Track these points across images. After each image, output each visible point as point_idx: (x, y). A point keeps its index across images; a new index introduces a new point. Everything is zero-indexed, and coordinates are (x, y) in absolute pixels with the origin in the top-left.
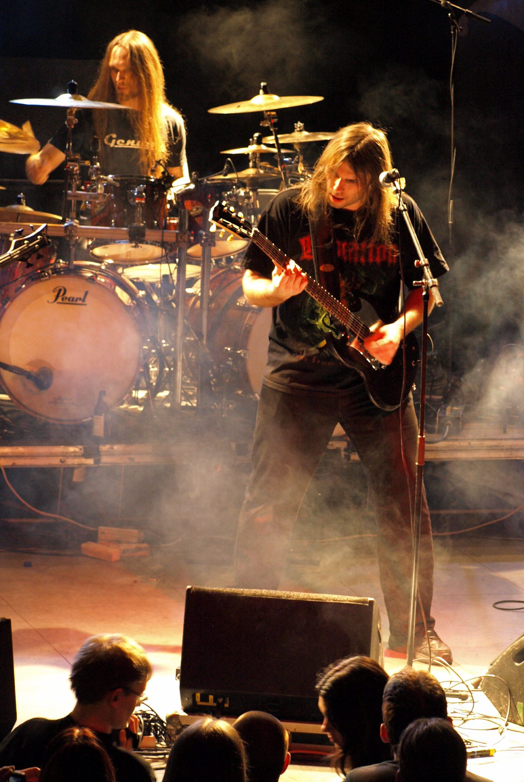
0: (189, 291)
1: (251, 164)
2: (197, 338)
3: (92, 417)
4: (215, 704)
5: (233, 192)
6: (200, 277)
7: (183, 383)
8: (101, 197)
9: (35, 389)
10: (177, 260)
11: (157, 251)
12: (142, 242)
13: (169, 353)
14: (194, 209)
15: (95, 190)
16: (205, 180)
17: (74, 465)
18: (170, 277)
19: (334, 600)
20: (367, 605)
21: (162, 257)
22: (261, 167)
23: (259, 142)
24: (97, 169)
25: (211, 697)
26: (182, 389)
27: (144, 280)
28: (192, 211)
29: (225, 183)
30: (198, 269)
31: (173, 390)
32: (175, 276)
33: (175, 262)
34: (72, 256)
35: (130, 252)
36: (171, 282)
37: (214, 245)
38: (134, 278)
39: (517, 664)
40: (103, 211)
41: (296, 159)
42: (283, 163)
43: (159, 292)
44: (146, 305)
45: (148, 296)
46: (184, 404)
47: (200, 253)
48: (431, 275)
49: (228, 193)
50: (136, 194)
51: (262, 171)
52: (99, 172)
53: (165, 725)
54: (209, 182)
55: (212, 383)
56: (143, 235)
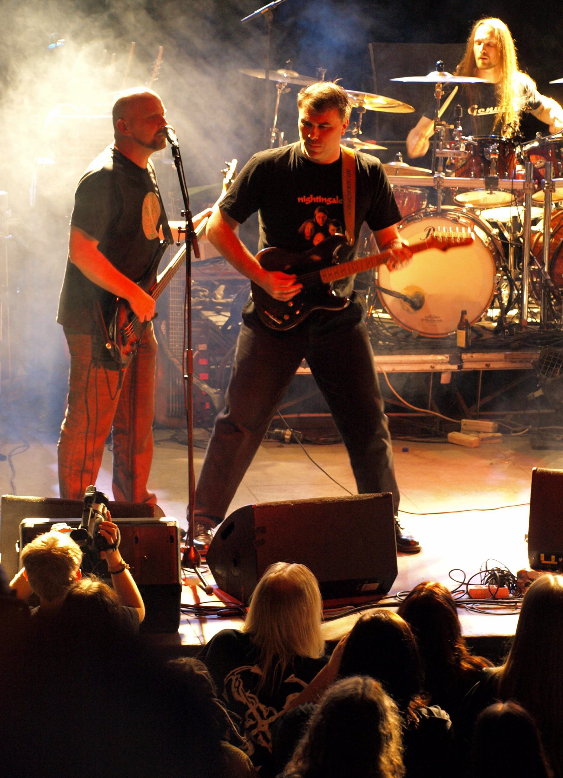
0: (534, 228)
2: (540, 267)
3: (456, 331)
4: (556, 563)
6: (543, 217)
7: (529, 303)
8: (462, 154)
9: (411, 310)
11: (508, 197)
12: (496, 189)
13: (518, 279)
14: (538, 163)
15: (458, 149)
16: (547, 139)
17: (441, 370)
18: (518, 217)
21: (512, 201)
24: (460, 131)
26: (529, 308)
28: (536, 164)
31: (521, 309)
32: (522, 218)
33: (522, 205)
34: (440, 202)
35: (486, 198)
36: (519, 221)
37: (554, 191)
40: (464, 165)
43: (509, 229)
44: (499, 241)
45: (501, 234)
46: (529, 320)
47: (543, 198)
50: (491, 151)
52: (461, 134)
53: (516, 579)
54: (549, 140)
55: (553, 303)
56: (497, 184)
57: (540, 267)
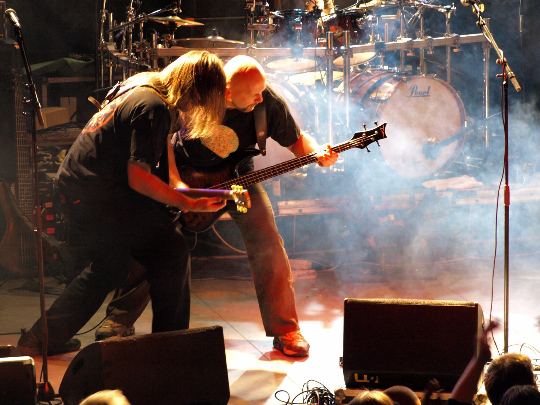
4: (368, 381)
5: (364, 17)
6: (343, 79)
8: (271, 27)
10: (326, 69)
15: (267, 22)
19: (450, 304)
20: (474, 307)
21: (316, 67)
24: (267, 7)
25: (365, 376)
27: (303, 84)
29: (358, 12)
32: (325, 80)
33: (325, 70)
37: (352, 57)
38: (297, 83)
47: (342, 63)
48: (509, 69)
49: (361, 19)
52: (268, 10)
53: (334, 397)
57: (343, 123)
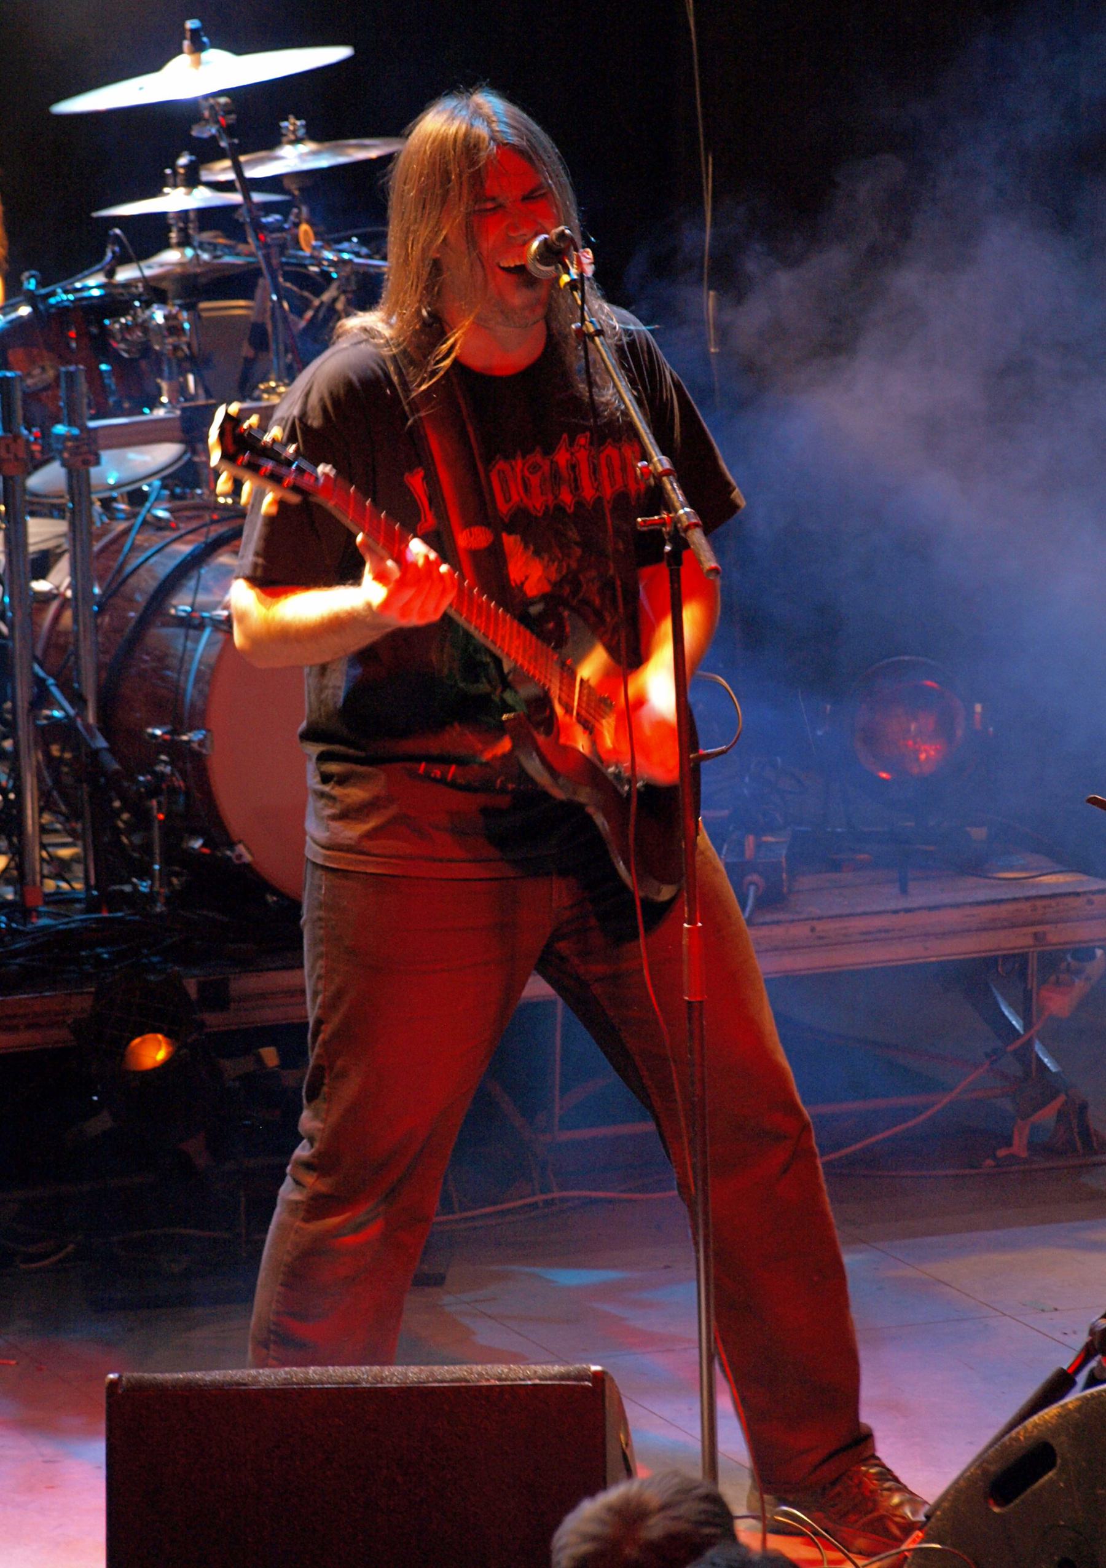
0: (40, 586)
1: (174, 236)
2: (72, 712)
5: (135, 317)
6: (66, 546)
7: (44, 830)
19: (500, 1380)
22: (201, 246)
23: (192, 180)
30: (61, 526)
37: (97, 462)
39: (996, 1510)
41: (292, 218)
42: (259, 227)
46: (50, 885)
49: (123, 320)
51: (205, 256)
55: (121, 825)
57: (72, 712)
